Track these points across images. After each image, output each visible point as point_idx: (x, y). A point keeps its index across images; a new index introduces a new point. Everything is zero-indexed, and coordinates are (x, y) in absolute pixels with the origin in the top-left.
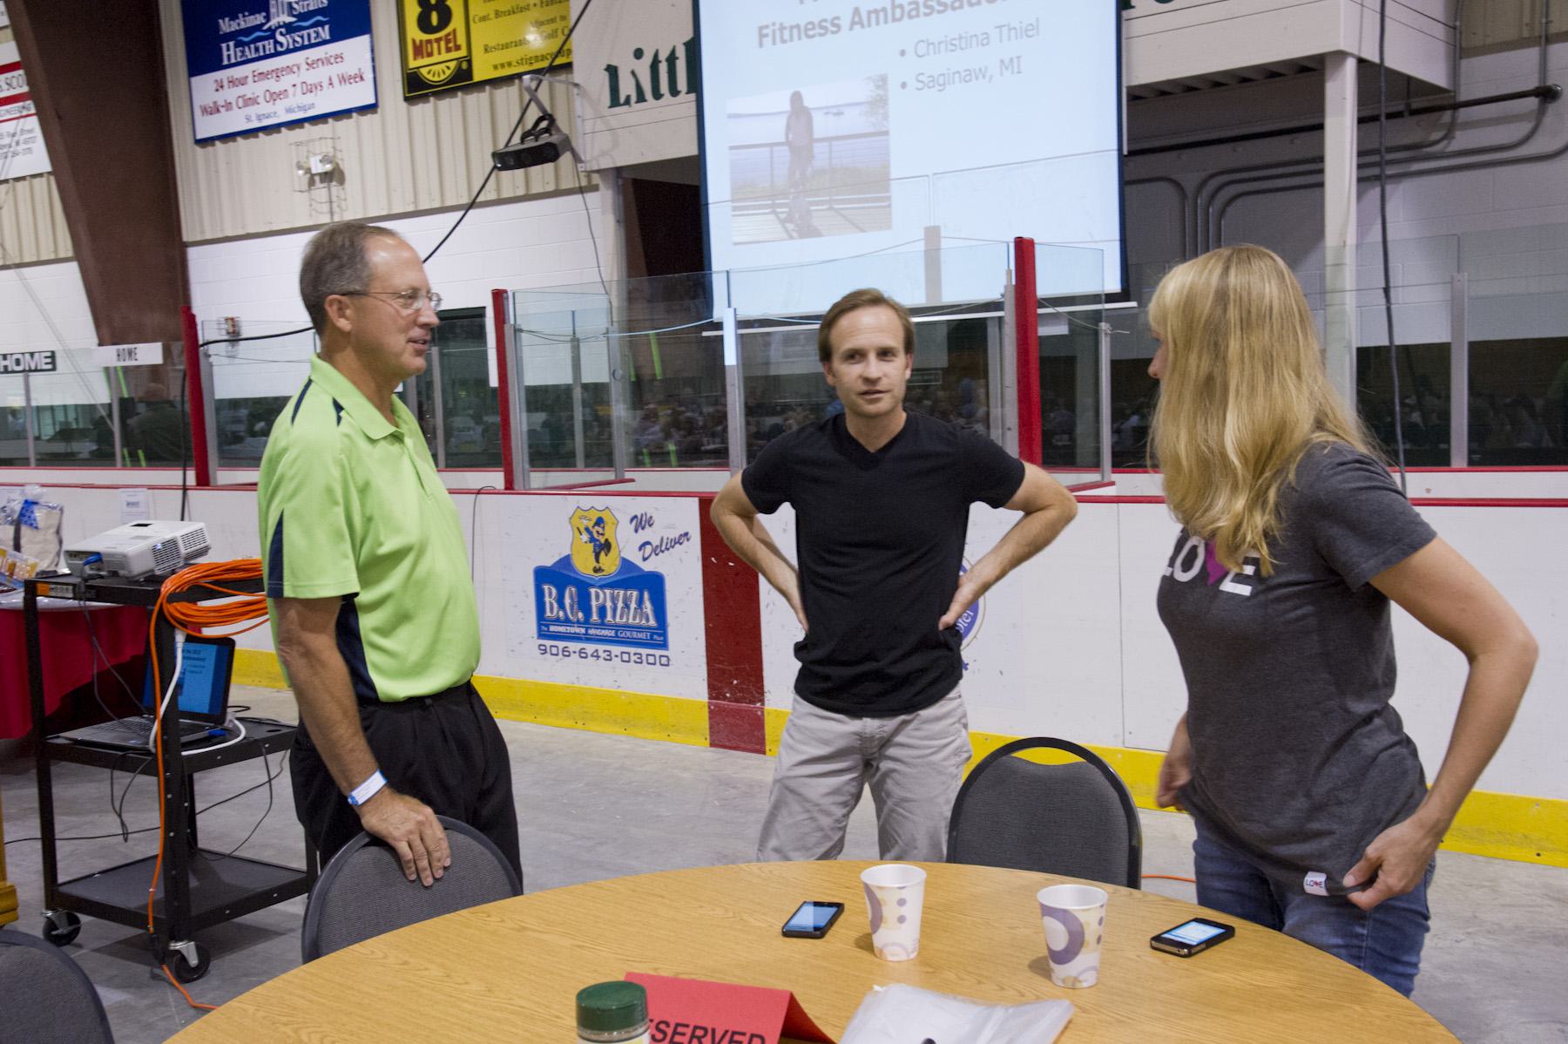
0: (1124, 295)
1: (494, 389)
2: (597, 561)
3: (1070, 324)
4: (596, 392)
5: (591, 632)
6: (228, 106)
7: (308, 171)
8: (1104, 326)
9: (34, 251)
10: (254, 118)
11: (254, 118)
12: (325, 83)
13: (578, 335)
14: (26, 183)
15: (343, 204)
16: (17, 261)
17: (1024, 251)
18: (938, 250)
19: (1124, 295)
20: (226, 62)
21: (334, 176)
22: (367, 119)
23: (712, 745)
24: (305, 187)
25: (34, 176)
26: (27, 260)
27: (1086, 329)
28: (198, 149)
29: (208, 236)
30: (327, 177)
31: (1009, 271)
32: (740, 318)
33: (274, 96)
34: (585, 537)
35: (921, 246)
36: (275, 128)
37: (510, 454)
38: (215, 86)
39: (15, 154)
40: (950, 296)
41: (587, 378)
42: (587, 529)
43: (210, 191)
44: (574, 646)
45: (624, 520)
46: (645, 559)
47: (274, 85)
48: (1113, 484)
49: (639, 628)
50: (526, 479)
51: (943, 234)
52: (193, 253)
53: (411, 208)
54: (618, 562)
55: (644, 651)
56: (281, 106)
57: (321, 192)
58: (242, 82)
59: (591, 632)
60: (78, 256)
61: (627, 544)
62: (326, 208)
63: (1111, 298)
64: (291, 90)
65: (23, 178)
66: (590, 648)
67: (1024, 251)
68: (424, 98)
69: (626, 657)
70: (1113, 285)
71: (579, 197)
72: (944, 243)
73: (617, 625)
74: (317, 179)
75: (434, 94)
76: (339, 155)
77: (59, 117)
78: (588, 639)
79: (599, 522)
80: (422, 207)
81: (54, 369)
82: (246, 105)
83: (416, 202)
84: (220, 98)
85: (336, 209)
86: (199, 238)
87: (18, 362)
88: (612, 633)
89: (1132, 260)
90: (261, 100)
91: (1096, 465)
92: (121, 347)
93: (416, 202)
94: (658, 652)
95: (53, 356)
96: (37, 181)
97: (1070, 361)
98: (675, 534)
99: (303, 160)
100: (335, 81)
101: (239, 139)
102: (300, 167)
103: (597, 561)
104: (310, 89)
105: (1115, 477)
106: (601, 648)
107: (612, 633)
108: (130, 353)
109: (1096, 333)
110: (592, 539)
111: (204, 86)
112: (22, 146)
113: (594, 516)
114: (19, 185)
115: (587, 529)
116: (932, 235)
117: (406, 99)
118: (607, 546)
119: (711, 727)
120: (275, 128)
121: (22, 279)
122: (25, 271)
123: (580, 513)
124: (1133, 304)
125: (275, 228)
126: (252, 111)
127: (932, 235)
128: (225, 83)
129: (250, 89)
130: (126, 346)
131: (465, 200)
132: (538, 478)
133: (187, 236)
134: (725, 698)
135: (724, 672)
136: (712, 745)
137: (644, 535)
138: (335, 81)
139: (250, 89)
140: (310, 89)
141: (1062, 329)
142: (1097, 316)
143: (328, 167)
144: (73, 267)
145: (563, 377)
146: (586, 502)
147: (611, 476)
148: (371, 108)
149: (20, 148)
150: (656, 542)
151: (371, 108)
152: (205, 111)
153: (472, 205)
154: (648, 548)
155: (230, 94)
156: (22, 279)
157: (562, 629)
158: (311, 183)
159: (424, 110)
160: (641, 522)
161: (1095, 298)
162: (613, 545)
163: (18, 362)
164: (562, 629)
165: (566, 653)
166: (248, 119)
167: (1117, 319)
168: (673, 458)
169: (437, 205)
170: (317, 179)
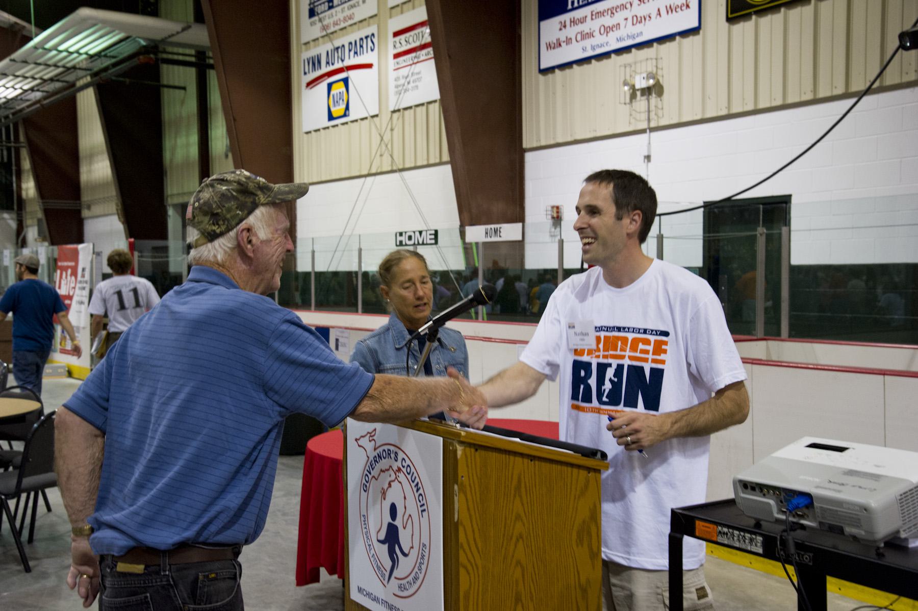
6: (568, 41)
7: (633, 87)
9: (425, 157)
10: (589, 48)
11: (589, 48)
12: (654, 14)
14: (412, 111)
15: (660, 113)
16: (401, 167)
20: (570, 7)
21: (655, 90)
22: (691, 39)
24: (628, 100)
25: (417, 106)
26: (407, 166)
28: (541, 77)
29: (543, 143)
30: (647, 91)
33: (607, 30)
36: (606, 55)
38: (559, 26)
39: (406, 91)
43: (547, 108)
47: (607, 21)
52: (529, 157)
56: (613, 35)
57: (641, 103)
58: (582, 20)
60: (452, 162)
62: (644, 116)
64: (623, 23)
65: (410, 108)
68: (747, 17)
74: (638, 93)
75: (757, 13)
76: (660, 72)
77: (450, 57)
80: (735, 110)
81: (436, 243)
82: (583, 38)
84: (562, 36)
85: (652, 115)
86: (535, 145)
87: (410, 238)
90: (596, 34)
92: (489, 227)
93: (729, 107)
95: (436, 233)
96: (419, 109)
99: (628, 78)
100: (663, 11)
101: (575, 66)
102: (625, 84)
104: (639, 20)
108: (496, 231)
111: (551, 28)
112: (412, 84)
114: (407, 112)
117: (729, 20)
120: (606, 55)
121: (403, 179)
122: (405, 174)
125: (599, 134)
126: (588, 43)
128: (568, 23)
129: (585, 27)
130: (493, 226)
133: (525, 146)
138: (663, 11)
139: (585, 27)
140: (639, 20)
143: (651, 82)
144: (448, 169)
148: (694, 31)
149: (410, 86)
151: (694, 31)
152: (549, 46)
155: (571, 32)
156: (403, 179)
158: (633, 96)
159: (745, 28)
163: (410, 238)
166: (584, 50)
169: (750, 107)
170: (638, 93)
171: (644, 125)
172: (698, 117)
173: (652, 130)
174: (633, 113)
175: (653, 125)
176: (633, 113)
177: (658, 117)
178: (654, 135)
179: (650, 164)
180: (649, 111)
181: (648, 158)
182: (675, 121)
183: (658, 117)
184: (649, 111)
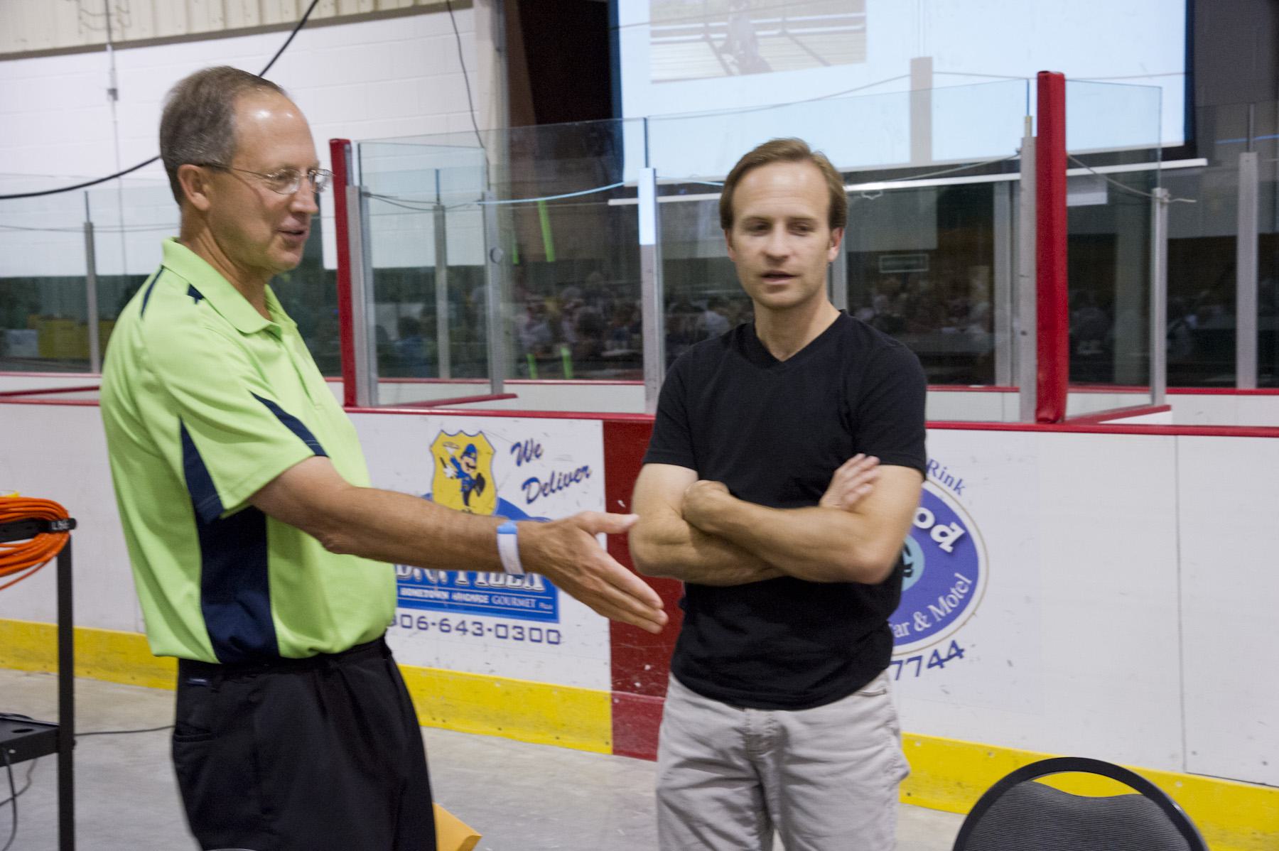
0: (1188, 150)
1: (331, 272)
2: (466, 502)
3: (1111, 190)
4: (467, 278)
5: (457, 597)
8: (1159, 192)
13: (444, 202)
17: (1051, 90)
18: (929, 90)
19: (1188, 150)
23: (617, 751)
27: (1133, 195)
31: (1028, 120)
32: (661, 181)
34: (451, 470)
35: (905, 85)
37: (353, 360)
40: (943, 153)
41: (456, 258)
42: (453, 461)
44: (433, 616)
45: (503, 448)
46: (530, 501)
48: (1166, 408)
49: (521, 593)
50: (373, 392)
51: (936, 67)
53: (218, 27)
54: (494, 504)
55: (527, 624)
59: (457, 597)
61: (506, 480)
62: (101, 22)
63: (1169, 153)
66: (454, 618)
67: (1051, 90)
69: (502, 631)
70: (1174, 136)
71: (445, 16)
72: (938, 81)
73: (491, 589)
78: (452, 606)
79: (470, 451)
80: (235, 24)
83: (225, 18)
88: (485, 599)
89: (1200, 101)
91: (1143, 382)
93: (225, 18)
94: (545, 626)
97: (1107, 242)
98: (570, 469)
103: (466, 502)
105: (1171, 399)
106: (470, 618)
107: (485, 599)
109: (1147, 204)
110: (460, 474)
113: (463, 443)
115: (453, 461)
116: (922, 69)
118: (479, 483)
119: (615, 728)
123: (444, 438)
124: (1202, 162)
127: (922, 69)
131: (292, 17)
132: (388, 392)
134: (634, 689)
135: (632, 651)
136: (617, 751)
137: (529, 469)
141: (1098, 197)
142: (1149, 180)
145: (423, 258)
146: (453, 424)
147: (485, 389)
150: (544, 479)
153: (302, 24)
154: (535, 486)
157: (417, 593)
160: (525, 452)
161: (1147, 155)
162: (488, 481)
164: (417, 593)
165: (422, 625)
167: (1176, 182)
168: (567, 367)
171: (101, 38)
172: (181, 31)
173: (117, 46)
174: (84, 15)
175: (116, 37)
176: (84, 15)
177: (123, 26)
178: (121, 55)
179: (117, 103)
180: (108, 14)
181: (113, 92)
182: (148, 35)
183: (123, 26)
184: (108, 14)
